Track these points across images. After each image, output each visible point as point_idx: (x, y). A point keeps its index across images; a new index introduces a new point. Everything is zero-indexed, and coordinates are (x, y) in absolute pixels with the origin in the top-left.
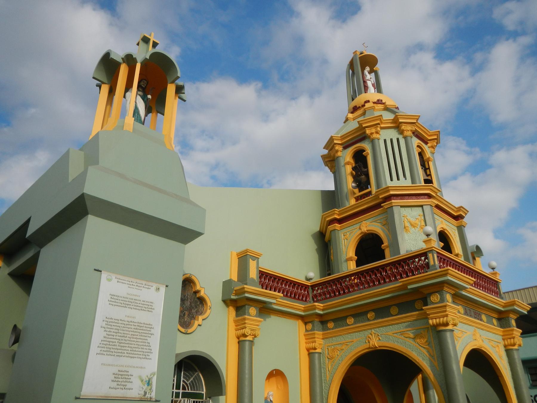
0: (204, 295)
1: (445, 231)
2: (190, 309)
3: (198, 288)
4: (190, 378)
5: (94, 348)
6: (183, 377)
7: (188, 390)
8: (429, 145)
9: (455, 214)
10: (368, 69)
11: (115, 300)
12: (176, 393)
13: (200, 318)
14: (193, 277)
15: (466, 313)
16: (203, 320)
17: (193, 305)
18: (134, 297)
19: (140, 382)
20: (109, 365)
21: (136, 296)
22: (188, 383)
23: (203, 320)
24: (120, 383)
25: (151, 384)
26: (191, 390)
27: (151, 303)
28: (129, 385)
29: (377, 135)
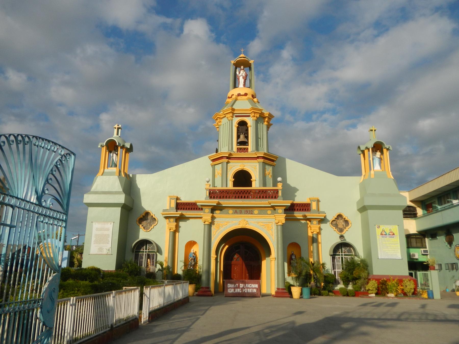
1: (244, 169)
2: (150, 222)
3: (152, 215)
4: (151, 246)
5: (92, 243)
6: (148, 246)
7: (150, 250)
8: (251, 116)
9: (256, 156)
11: (97, 229)
13: (153, 225)
15: (236, 213)
17: (151, 221)
18: (103, 228)
22: (150, 248)
23: (154, 226)
26: (152, 250)
28: (103, 251)
29: (219, 123)
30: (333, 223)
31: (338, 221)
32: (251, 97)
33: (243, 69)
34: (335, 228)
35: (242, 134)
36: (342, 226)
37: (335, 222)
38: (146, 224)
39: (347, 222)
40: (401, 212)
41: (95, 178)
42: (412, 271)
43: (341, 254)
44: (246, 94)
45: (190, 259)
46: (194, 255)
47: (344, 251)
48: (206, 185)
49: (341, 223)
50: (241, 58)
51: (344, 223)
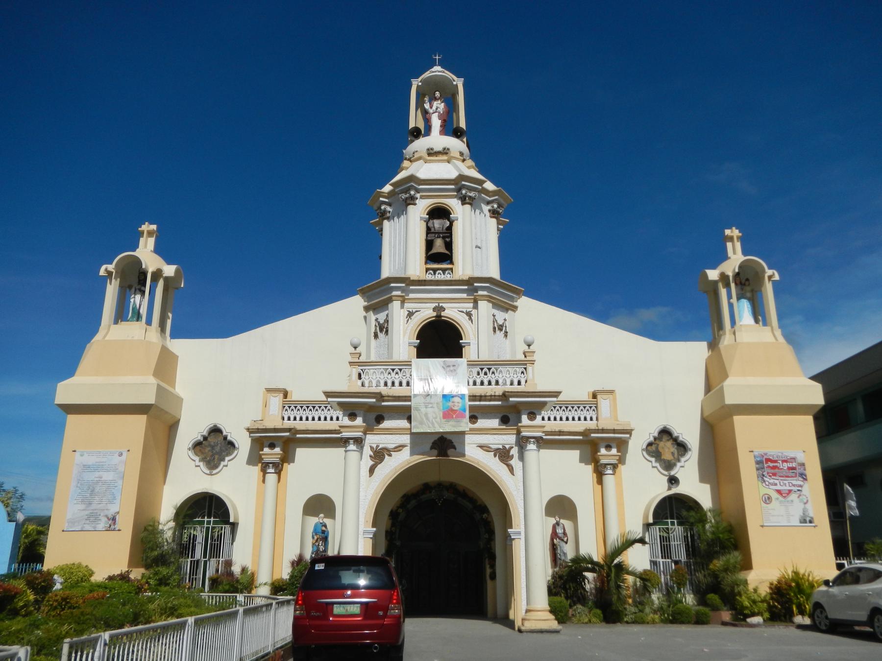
0: (231, 439)
3: (224, 433)
6: (214, 509)
10: (426, 99)
11: (86, 468)
12: (207, 521)
13: (227, 459)
14: (218, 425)
16: (229, 461)
19: (106, 519)
20: (83, 510)
21: (103, 462)
23: (229, 461)
24: (91, 521)
25: (116, 519)
27: (116, 465)
30: (649, 448)
31: (661, 444)
32: (458, 155)
33: (439, 99)
34: (656, 461)
35: (438, 237)
36: (671, 455)
37: (653, 448)
38: (211, 456)
39: (682, 447)
40: (809, 420)
41: (88, 345)
42: (843, 560)
43: (671, 522)
44: (445, 152)
45: (316, 538)
46: (324, 528)
47: (676, 513)
48: (350, 353)
49: (669, 448)
50: (435, 72)
51: (674, 449)
